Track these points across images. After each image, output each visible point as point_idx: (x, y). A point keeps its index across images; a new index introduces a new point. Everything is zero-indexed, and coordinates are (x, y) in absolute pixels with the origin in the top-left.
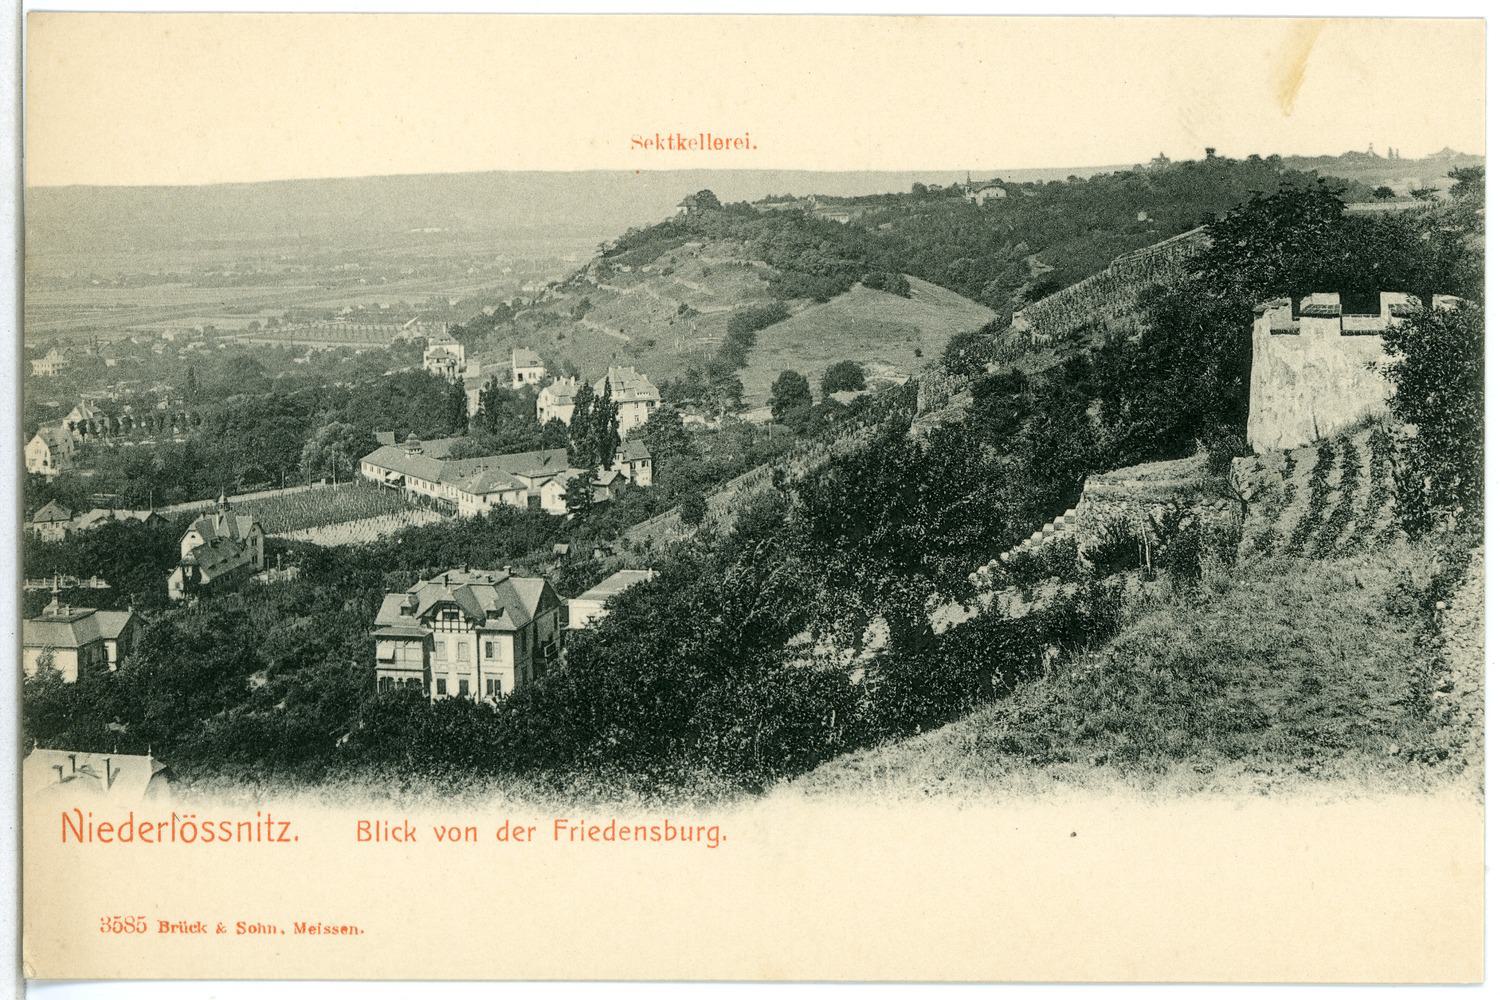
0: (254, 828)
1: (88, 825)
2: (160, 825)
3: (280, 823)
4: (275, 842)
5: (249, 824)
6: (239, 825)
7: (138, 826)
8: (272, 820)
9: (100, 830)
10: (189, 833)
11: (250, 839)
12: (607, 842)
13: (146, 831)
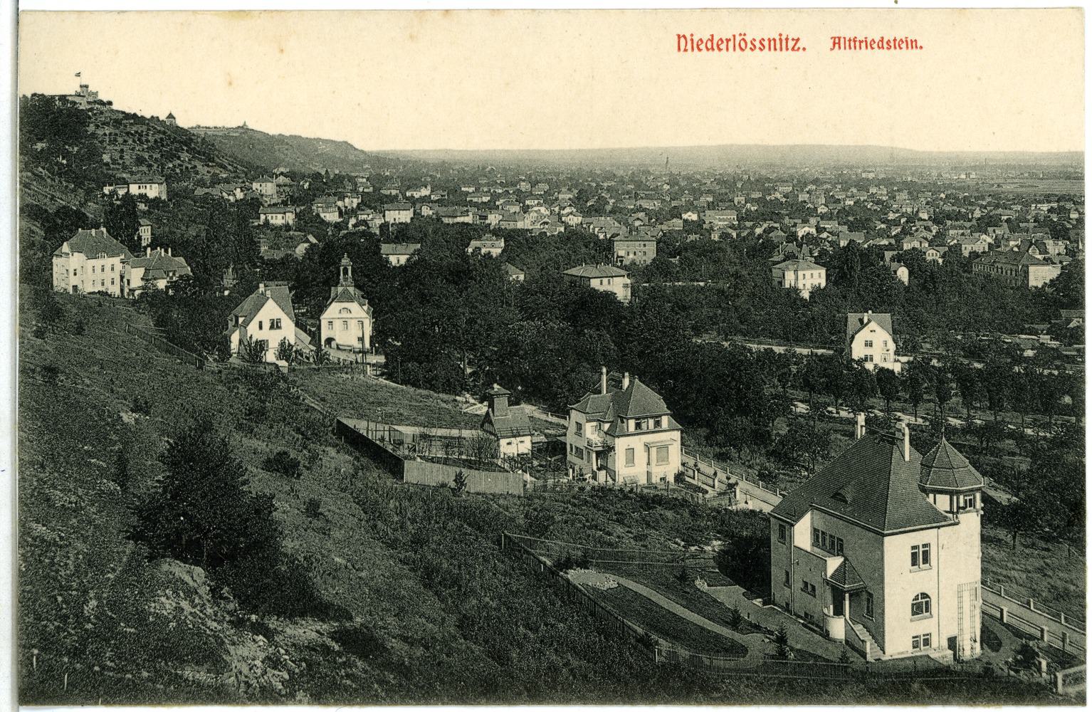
0: (778, 42)
6: (769, 40)
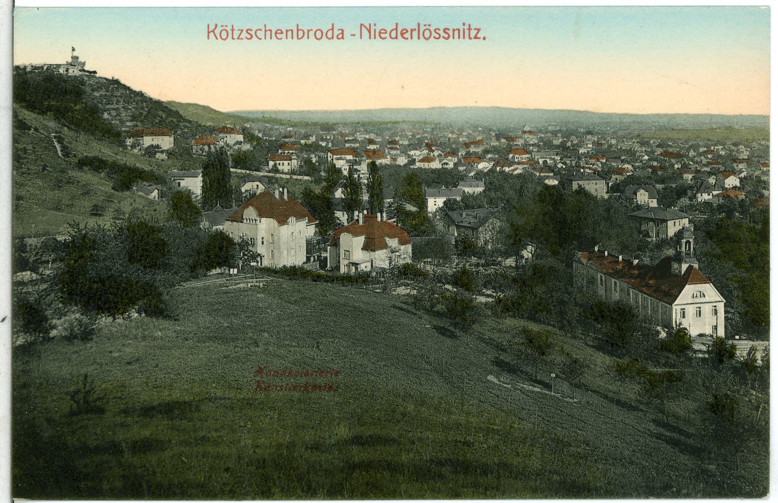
1: (373, 30)
2: (412, 30)
3: (475, 29)
5: (459, 30)
6: (454, 30)
7: (423, 31)
8: (471, 28)
9: (380, 33)
10: (427, 34)
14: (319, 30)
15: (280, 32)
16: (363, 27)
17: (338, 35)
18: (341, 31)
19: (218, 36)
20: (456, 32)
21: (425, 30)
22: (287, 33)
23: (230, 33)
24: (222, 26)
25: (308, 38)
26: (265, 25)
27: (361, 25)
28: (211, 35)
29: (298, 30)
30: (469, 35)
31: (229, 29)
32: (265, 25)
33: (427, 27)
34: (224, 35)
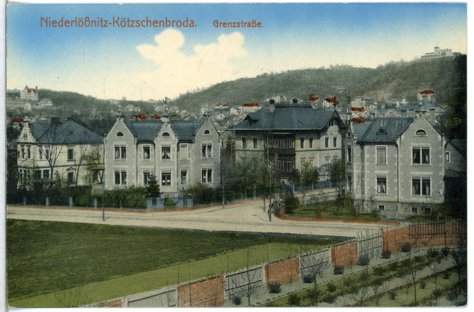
4: (104, 28)
8: (103, 20)
9: (53, 23)
11: (95, 26)
12: (185, 28)
13: (67, 23)
14: (179, 21)
15: (55, 22)
16: (43, 20)
17: (190, 24)
18: (192, 22)
19: (120, 25)
20: (94, 23)
21: (80, 21)
22: (160, 23)
23: (127, 23)
24: (122, 19)
25: (92, 26)
26: (147, 18)
27: (42, 18)
28: (116, 24)
29: (167, 21)
30: (101, 24)
31: (126, 20)
32: (147, 18)
33: (123, 20)
34: (123, 24)
